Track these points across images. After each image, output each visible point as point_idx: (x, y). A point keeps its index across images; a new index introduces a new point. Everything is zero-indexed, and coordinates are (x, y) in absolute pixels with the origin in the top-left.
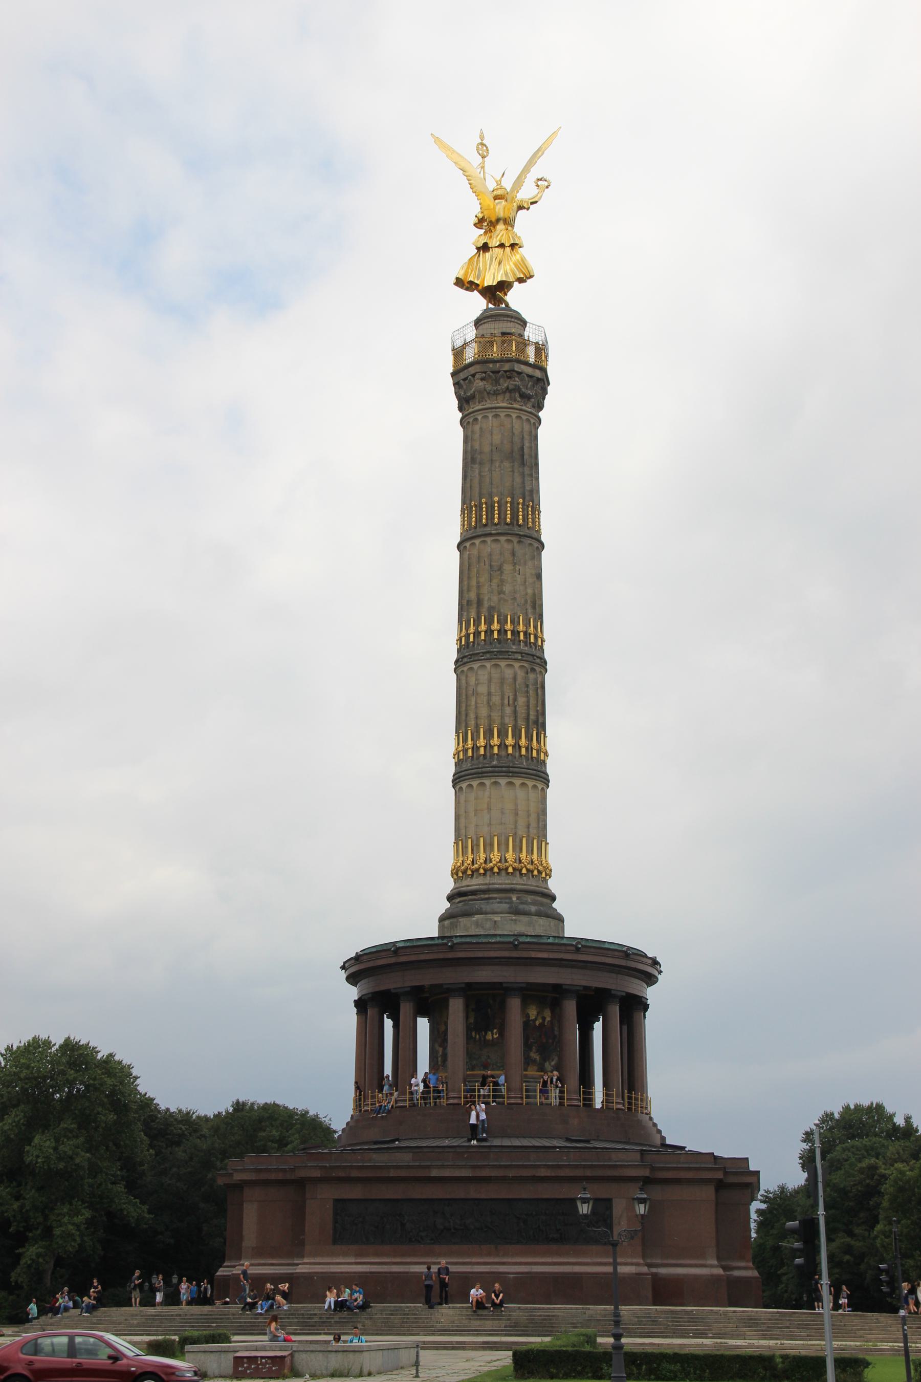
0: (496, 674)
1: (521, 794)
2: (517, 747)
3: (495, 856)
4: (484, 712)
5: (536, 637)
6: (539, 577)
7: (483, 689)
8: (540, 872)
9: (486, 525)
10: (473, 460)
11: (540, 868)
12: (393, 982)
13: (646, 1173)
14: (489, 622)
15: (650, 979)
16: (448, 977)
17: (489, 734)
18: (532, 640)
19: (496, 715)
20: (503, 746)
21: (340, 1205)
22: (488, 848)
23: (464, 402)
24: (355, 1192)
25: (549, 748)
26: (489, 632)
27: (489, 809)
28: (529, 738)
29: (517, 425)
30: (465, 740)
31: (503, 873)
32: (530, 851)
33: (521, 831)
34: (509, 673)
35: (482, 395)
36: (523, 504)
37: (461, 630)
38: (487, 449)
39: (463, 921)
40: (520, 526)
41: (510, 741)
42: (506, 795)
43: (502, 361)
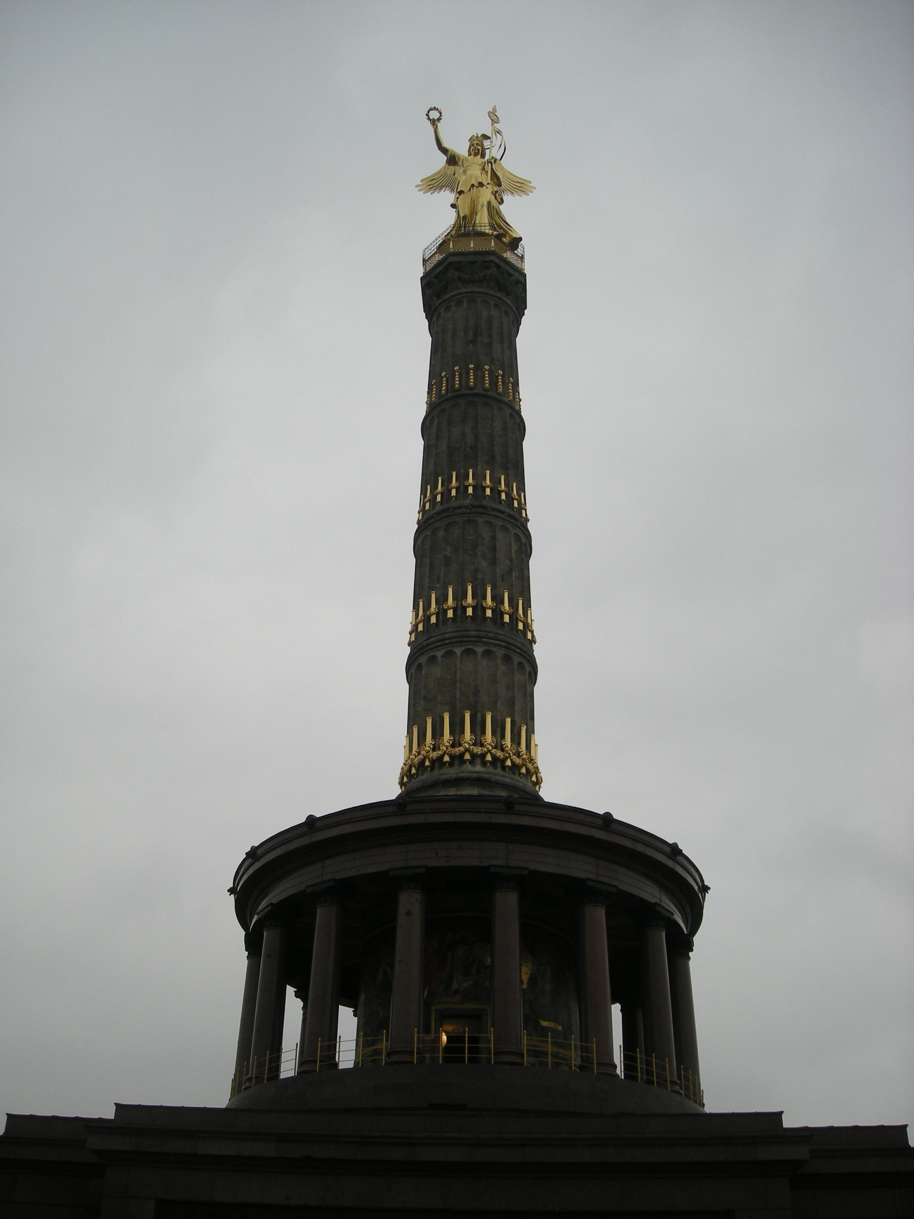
5: (519, 503)
8: (528, 770)
9: (459, 390)
11: (530, 766)
15: (695, 918)
18: (516, 504)
22: (458, 731)
25: (535, 627)
26: (461, 489)
28: (513, 604)
30: (427, 606)
31: (478, 761)
32: (516, 739)
36: (503, 376)
37: (425, 497)
40: (498, 394)
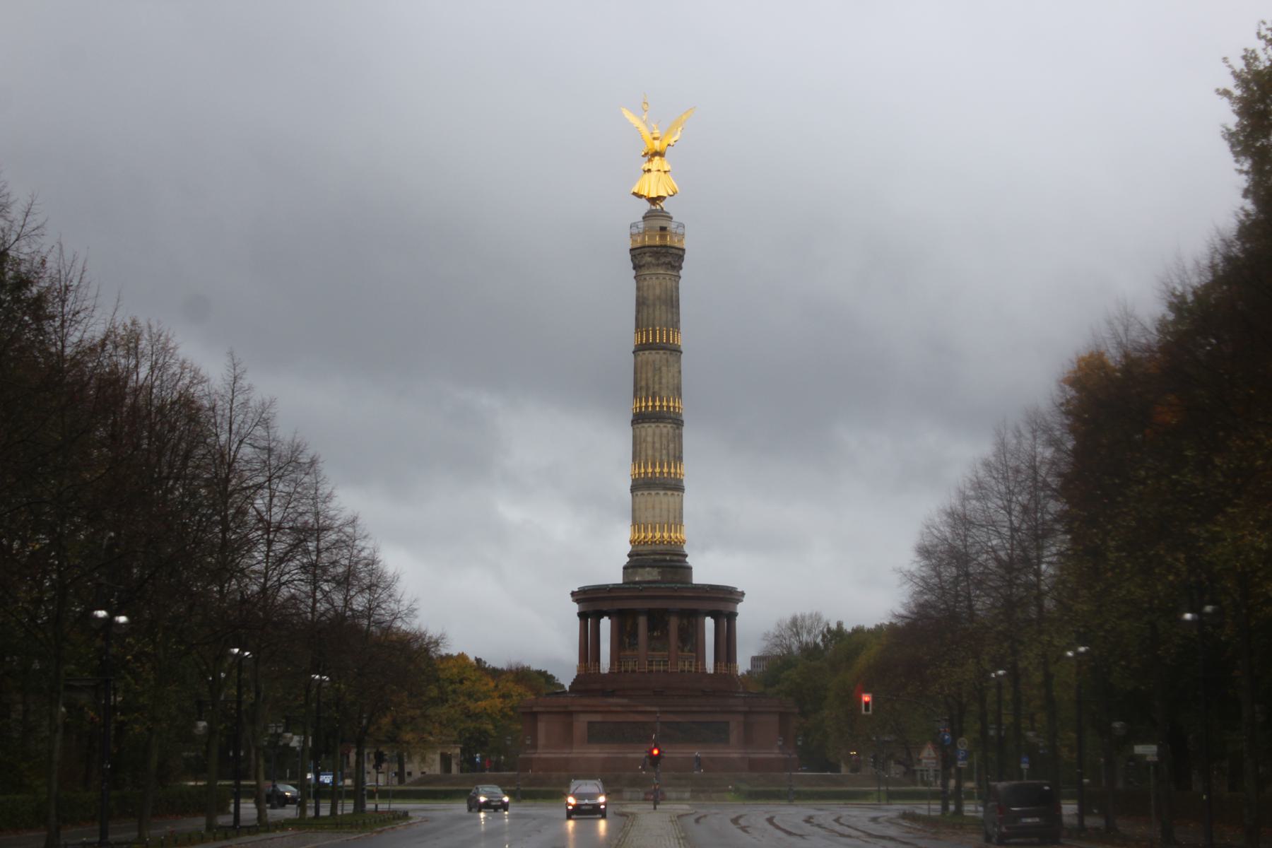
0: (658, 431)
1: (671, 499)
2: (669, 473)
3: (658, 535)
4: (650, 452)
6: (680, 372)
7: (649, 439)
10: (644, 303)
12: (605, 606)
13: (746, 709)
14: (654, 401)
16: (637, 605)
17: (654, 466)
19: (657, 455)
20: (661, 473)
21: (589, 723)
23: (636, 267)
24: (597, 718)
26: (653, 406)
27: (654, 508)
29: (669, 283)
33: (671, 520)
34: (665, 431)
35: (648, 265)
38: (651, 298)
39: (640, 570)
41: (665, 470)
42: (663, 499)
43: (661, 246)
